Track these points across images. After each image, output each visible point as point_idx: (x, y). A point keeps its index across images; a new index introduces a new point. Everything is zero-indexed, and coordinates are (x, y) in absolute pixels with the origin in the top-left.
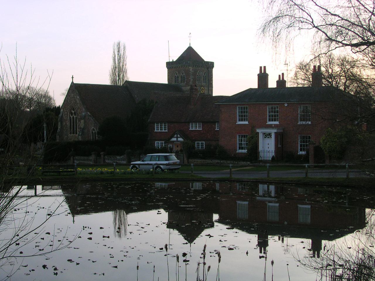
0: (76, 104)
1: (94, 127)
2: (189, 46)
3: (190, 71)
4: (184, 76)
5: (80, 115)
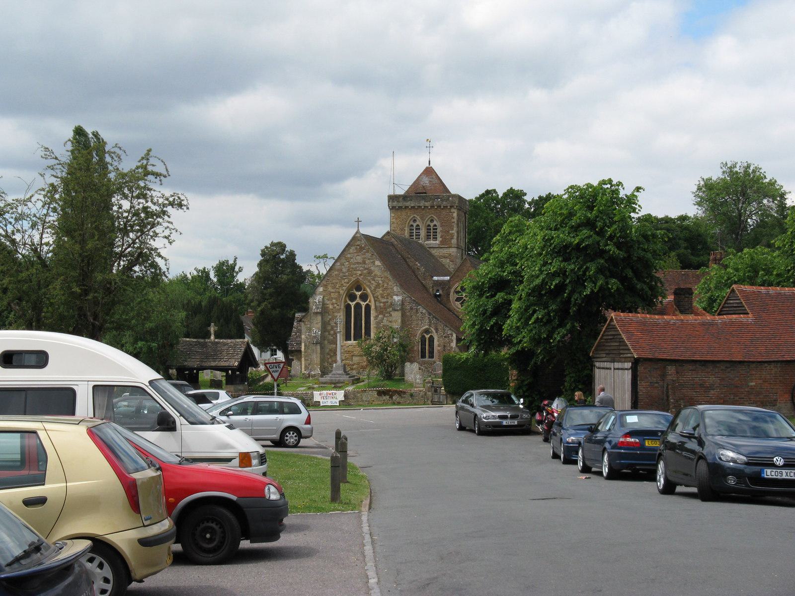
0: (369, 278)
1: (430, 326)
2: (428, 165)
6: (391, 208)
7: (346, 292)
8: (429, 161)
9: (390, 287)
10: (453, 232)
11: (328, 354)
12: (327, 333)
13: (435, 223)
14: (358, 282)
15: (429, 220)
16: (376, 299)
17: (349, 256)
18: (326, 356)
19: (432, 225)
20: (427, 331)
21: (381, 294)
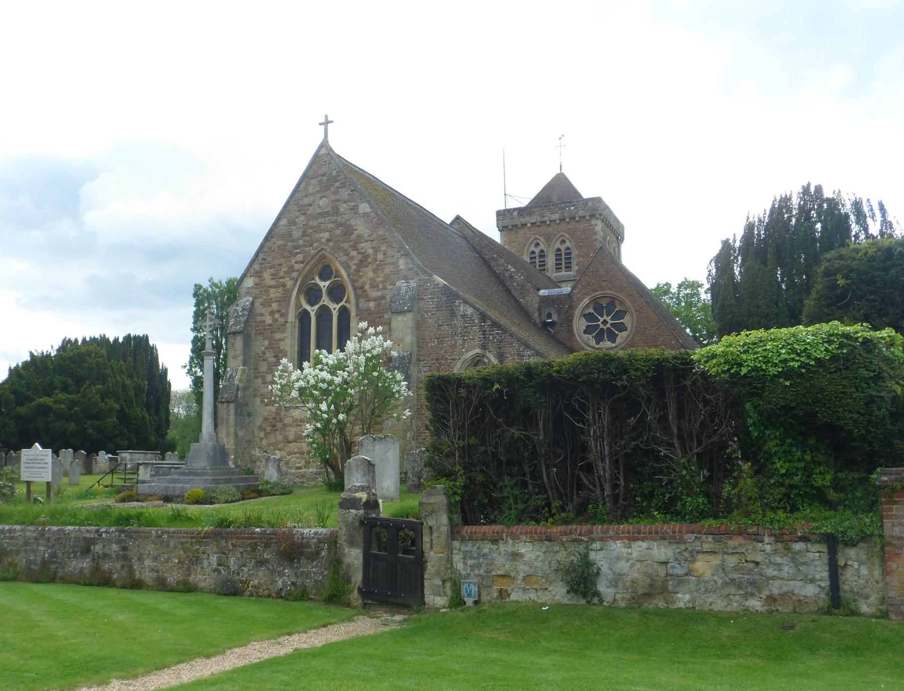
0: (346, 246)
1: (484, 347)
2: (559, 172)
3: (595, 233)
4: (568, 248)
5: (373, 294)
6: (501, 228)
7: (299, 283)
8: (561, 166)
9: (389, 260)
11: (262, 429)
12: (260, 380)
13: (568, 244)
14: (324, 257)
15: (559, 242)
16: (360, 292)
17: (306, 201)
18: (256, 434)
19: (563, 248)
21: (370, 279)
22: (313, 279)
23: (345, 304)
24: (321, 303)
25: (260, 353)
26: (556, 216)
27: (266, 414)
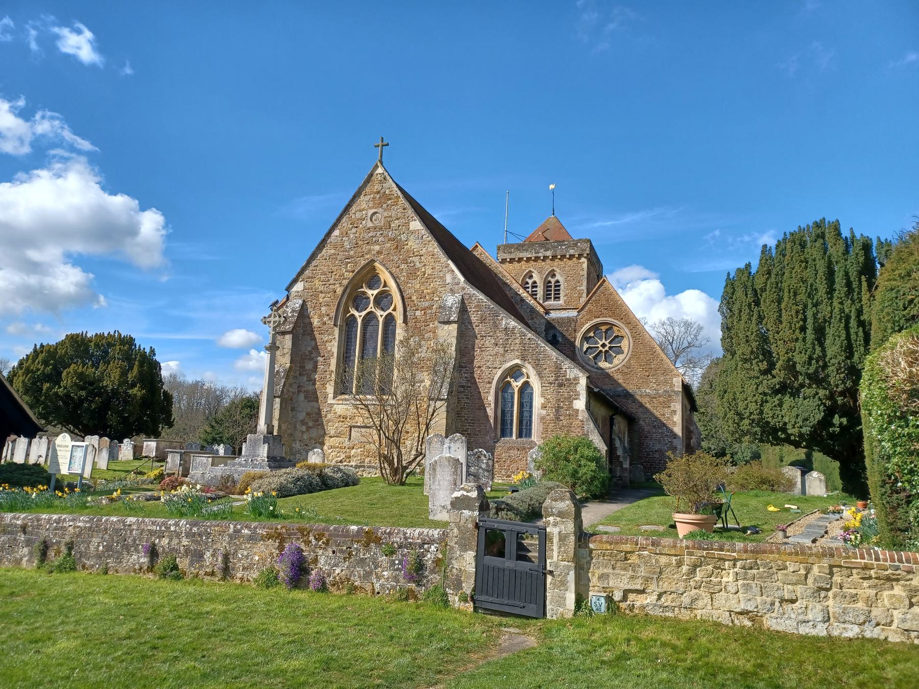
7: (348, 290)
10: (582, 288)
11: (303, 422)
12: (305, 378)
20: (515, 372)
22: (362, 287)
23: (392, 312)
24: (368, 310)
25: (307, 352)
26: (549, 253)
27: (309, 410)
